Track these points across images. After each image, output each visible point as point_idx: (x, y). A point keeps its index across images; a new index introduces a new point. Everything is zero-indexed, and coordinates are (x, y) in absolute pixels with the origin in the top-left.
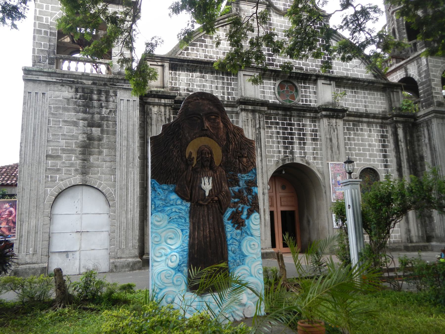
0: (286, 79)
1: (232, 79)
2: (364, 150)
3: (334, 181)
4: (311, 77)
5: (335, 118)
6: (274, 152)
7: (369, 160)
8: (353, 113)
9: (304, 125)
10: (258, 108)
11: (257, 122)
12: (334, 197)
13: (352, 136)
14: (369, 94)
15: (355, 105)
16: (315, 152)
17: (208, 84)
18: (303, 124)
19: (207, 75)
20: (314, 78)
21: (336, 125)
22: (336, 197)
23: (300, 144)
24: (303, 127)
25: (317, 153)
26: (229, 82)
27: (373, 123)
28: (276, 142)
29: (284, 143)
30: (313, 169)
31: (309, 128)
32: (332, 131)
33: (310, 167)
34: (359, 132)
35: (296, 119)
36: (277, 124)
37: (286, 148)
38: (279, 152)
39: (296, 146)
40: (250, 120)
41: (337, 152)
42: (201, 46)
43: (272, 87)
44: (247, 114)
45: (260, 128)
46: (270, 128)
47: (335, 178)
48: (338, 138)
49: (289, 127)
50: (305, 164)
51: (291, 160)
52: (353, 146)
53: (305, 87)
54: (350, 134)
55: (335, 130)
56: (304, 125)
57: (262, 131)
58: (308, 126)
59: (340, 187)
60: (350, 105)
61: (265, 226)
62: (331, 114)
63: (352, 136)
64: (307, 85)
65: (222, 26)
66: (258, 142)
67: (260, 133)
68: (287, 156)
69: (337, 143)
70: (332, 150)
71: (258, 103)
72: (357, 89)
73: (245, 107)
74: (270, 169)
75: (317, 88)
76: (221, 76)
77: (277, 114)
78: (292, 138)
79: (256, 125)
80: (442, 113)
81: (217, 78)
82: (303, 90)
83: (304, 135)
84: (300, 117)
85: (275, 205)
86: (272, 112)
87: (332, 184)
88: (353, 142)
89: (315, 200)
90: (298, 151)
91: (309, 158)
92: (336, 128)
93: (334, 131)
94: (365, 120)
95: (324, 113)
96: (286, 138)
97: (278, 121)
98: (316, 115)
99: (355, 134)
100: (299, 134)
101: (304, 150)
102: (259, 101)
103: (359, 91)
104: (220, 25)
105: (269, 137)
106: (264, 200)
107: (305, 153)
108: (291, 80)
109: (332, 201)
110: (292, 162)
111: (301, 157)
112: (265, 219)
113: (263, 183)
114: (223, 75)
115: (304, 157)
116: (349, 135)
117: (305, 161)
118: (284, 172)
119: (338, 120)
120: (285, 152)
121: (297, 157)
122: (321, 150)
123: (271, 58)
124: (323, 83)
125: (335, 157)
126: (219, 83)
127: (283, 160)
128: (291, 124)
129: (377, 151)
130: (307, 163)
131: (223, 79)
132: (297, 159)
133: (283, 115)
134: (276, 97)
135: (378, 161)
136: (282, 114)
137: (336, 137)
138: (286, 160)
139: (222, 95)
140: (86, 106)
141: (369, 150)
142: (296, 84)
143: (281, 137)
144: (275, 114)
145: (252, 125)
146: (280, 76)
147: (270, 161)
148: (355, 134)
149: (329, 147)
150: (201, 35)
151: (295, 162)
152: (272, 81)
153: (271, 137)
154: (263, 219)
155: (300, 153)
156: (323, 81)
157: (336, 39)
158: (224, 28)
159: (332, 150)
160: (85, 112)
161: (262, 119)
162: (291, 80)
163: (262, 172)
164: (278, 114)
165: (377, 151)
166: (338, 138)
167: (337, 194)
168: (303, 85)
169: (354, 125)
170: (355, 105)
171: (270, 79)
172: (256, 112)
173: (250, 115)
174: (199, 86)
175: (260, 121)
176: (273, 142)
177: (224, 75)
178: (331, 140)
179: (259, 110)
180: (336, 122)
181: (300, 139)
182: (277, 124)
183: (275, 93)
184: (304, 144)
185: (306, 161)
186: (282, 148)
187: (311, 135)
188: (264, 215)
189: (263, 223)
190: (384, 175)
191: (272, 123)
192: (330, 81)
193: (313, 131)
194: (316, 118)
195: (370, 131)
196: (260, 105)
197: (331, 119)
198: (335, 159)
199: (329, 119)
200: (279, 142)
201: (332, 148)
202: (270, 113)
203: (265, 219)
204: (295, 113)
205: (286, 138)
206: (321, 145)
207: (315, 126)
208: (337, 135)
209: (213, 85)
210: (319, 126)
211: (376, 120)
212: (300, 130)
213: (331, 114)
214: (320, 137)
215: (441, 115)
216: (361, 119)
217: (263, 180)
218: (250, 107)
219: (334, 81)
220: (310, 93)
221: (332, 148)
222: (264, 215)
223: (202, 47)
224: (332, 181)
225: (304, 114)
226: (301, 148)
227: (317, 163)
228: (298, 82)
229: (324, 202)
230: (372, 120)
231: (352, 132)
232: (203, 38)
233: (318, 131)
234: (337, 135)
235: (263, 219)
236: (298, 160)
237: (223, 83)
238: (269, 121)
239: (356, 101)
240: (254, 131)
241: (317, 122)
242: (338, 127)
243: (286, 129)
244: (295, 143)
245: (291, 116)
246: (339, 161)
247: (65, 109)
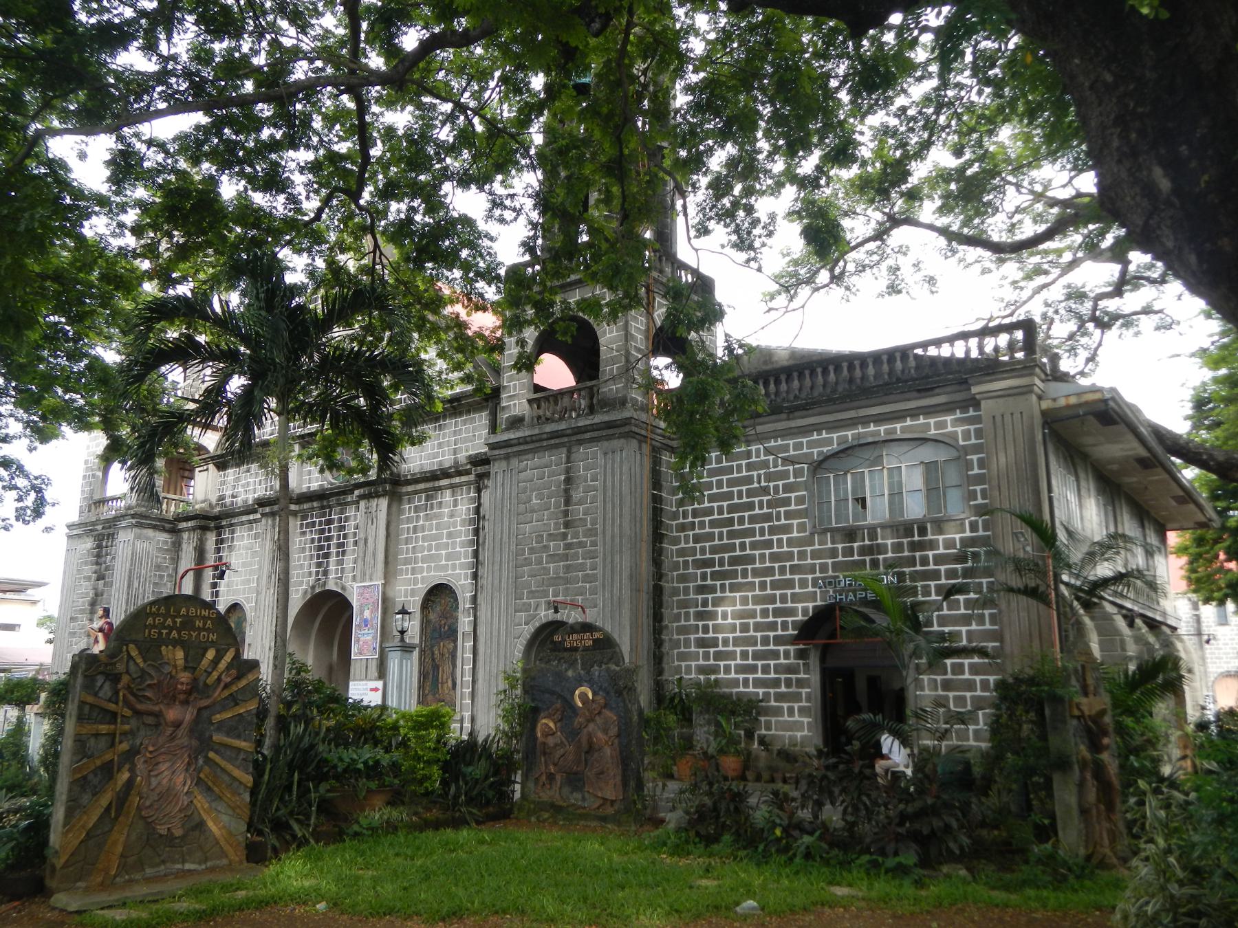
2: (438, 547)
7: (445, 568)
9: (347, 518)
14: (465, 423)
27: (460, 485)
33: (346, 595)
36: (313, 524)
37: (319, 565)
39: (333, 559)
46: (304, 533)
47: (362, 613)
78: (329, 548)
80: (500, 448)
94: (443, 482)
99: (427, 518)
107: (342, 571)
115: (341, 578)
127: (313, 587)
129: (463, 545)
130: (343, 588)
135: (462, 566)
140: (98, 556)
141: (446, 546)
160: (97, 563)
164: (313, 509)
165: (463, 545)
169: (427, 499)
174: (243, 486)
184: (344, 553)
190: (468, 595)
191: (308, 526)
195: (455, 503)
204: (333, 500)
211: (464, 479)
215: (502, 451)
216: (437, 484)
218: (267, 510)
230: (456, 480)
236: (331, 586)
245: (330, 507)
246: (371, 580)
247: (86, 563)
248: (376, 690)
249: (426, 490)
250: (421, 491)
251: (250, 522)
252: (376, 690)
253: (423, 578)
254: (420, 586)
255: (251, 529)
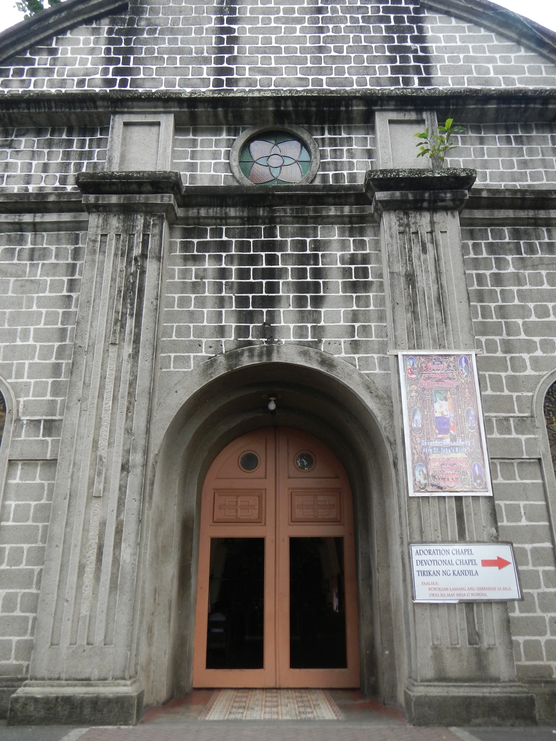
0: (270, 126)
1: (95, 144)
3: (418, 417)
4: (347, 106)
5: (428, 209)
6: (200, 332)
8: (508, 195)
10: (140, 198)
11: (138, 239)
12: (420, 478)
13: (511, 269)
15: (523, 176)
16: (357, 325)
17: (19, 162)
18: (315, 242)
19: (23, 139)
20: (358, 108)
21: (431, 232)
22: (426, 477)
23: (300, 302)
24: (315, 249)
25: (365, 330)
26: (87, 149)
28: (210, 302)
29: (242, 302)
30: (346, 381)
31: (339, 254)
32: (416, 249)
34: (539, 255)
35: (290, 228)
36: (224, 246)
38: (221, 331)
40: (112, 235)
41: (437, 315)
42: (19, 73)
43: (223, 150)
44: (105, 220)
45: (144, 256)
46: (196, 259)
48: (438, 272)
49: (263, 254)
50: (315, 366)
51: (261, 355)
52: (516, 302)
53: (333, 142)
54: (500, 263)
55: (429, 246)
56: (317, 245)
57: (151, 266)
58: (335, 245)
59: (447, 441)
60: (502, 177)
61: (114, 586)
62: (410, 197)
63: (511, 269)
64: (344, 135)
65: (89, 21)
66: (132, 300)
67: (143, 272)
68: (250, 343)
69: (434, 288)
70: (414, 312)
71: (140, 184)
72: (527, 128)
73: (97, 199)
74: (178, 387)
75: (374, 141)
76: (64, 137)
77: (221, 218)
78: (272, 287)
79: (131, 249)
81: (50, 144)
82: (328, 149)
83: (317, 273)
84: (305, 220)
85: (270, 519)
86: (203, 212)
87: (412, 430)
88: (515, 289)
89: (375, 496)
90: (292, 326)
91: (333, 346)
92: (434, 242)
93: (424, 250)
95: (380, 195)
96: (251, 288)
97: (224, 238)
98: (363, 210)
99: (522, 263)
100: (301, 273)
101: (317, 320)
102: (143, 177)
103: (534, 134)
104: (80, 19)
105: (189, 287)
106: (122, 489)
107: (318, 331)
108: (287, 127)
109: (411, 494)
110: (265, 360)
111: (300, 344)
112: (116, 560)
113: (129, 431)
114: (70, 133)
115: (316, 344)
116: (498, 268)
117: (316, 357)
118: (272, 406)
119: (439, 217)
120: (242, 332)
121: (288, 343)
122: (381, 317)
123: (224, 78)
124: (391, 122)
125: (426, 332)
126: (54, 156)
127: (233, 356)
128: (271, 246)
130: (325, 361)
131: (69, 143)
132: (284, 349)
133: (243, 220)
134: (233, 176)
136: (241, 218)
137: (431, 268)
138: (242, 354)
139: (57, 184)
142: (305, 136)
143: (230, 286)
144: (216, 218)
145: (117, 249)
146: (247, 118)
147: (182, 361)
148: (522, 263)
149: (403, 301)
150: (19, 48)
151: (275, 359)
152: (224, 136)
153: (196, 287)
154: (108, 559)
155: (301, 332)
156: (394, 116)
157: (445, 8)
158: (94, 26)
159: (414, 312)
161: (156, 231)
162: (287, 127)
163: (131, 394)
164: (224, 219)
166: (438, 272)
167: (434, 466)
168: (327, 135)
169: (516, 235)
170: (523, 176)
171: (217, 131)
172: (137, 211)
173: (115, 222)
175: (146, 236)
176: (201, 302)
177: (75, 133)
178: (411, 279)
179: (146, 205)
180: (432, 223)
181: (301, 287)
182: (224, 246)
183: (229, 167)
184: (318, 302)
185: (321, 354)
186: (233, 319)
187: (346, 273)
188: (117, 545)
189: (106, 578)
191: (203, 246)
192: (419, 111)
193: (353, 259)
194: (362, 219)
196: (149, 188)
197: (412, 214)
198: (427, 339)
199: (407, 214)
200: (221, 302)
201: (413, 306)
202: (198, 218)
203: (116, 560)
205: (251, 288)
206: (381, 302)
207: (361, 244)
208: (437, 261)
209: (34, 163)
210: (377, 244)
212: (303, 259)
213: (410, 197)
214: (381, 276)
216: (542, 214)
217: (129, 417)
218: (114, 199)
219: (431, 110)
220: (351, 154)
221: (413, 306)
222: (117, 545)
223: (22, 75)
224: (411, 419)
225: (315, 211)
226: (302, 317)
227: (366, 363)
228: (310, 131)
229: (395, 501)
231: (509, 258)
232: (28, 55)
233: (373, 259)
234: (437, 261)
235: (108, 559)
237: (67, 155)
238: (195, 241)
239: (524, 164)
240: (122, 265)
241: (370, 231)
242: (439, 237)
243: (254, 260)
244: (283, 301)
245: (272, 221)
246: (441, 346)
248: (500, 563)
249: (514, 222)
250: (503, 222)
251: (20, 227)
252: (500, 563)
253: (535, 362)
254: (529, 372)
255: (21, 241)
